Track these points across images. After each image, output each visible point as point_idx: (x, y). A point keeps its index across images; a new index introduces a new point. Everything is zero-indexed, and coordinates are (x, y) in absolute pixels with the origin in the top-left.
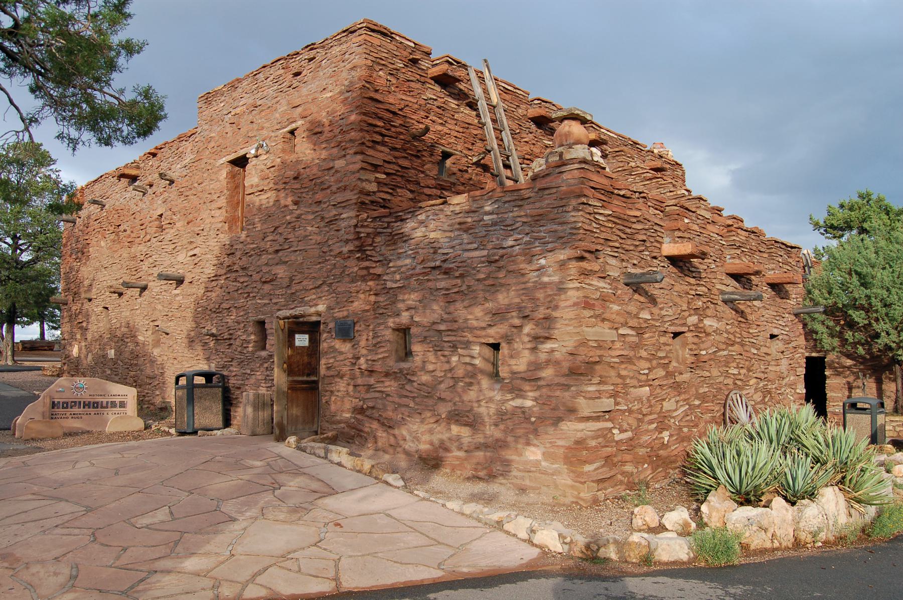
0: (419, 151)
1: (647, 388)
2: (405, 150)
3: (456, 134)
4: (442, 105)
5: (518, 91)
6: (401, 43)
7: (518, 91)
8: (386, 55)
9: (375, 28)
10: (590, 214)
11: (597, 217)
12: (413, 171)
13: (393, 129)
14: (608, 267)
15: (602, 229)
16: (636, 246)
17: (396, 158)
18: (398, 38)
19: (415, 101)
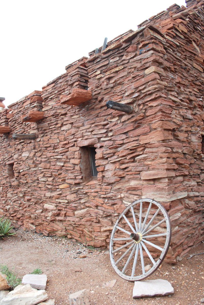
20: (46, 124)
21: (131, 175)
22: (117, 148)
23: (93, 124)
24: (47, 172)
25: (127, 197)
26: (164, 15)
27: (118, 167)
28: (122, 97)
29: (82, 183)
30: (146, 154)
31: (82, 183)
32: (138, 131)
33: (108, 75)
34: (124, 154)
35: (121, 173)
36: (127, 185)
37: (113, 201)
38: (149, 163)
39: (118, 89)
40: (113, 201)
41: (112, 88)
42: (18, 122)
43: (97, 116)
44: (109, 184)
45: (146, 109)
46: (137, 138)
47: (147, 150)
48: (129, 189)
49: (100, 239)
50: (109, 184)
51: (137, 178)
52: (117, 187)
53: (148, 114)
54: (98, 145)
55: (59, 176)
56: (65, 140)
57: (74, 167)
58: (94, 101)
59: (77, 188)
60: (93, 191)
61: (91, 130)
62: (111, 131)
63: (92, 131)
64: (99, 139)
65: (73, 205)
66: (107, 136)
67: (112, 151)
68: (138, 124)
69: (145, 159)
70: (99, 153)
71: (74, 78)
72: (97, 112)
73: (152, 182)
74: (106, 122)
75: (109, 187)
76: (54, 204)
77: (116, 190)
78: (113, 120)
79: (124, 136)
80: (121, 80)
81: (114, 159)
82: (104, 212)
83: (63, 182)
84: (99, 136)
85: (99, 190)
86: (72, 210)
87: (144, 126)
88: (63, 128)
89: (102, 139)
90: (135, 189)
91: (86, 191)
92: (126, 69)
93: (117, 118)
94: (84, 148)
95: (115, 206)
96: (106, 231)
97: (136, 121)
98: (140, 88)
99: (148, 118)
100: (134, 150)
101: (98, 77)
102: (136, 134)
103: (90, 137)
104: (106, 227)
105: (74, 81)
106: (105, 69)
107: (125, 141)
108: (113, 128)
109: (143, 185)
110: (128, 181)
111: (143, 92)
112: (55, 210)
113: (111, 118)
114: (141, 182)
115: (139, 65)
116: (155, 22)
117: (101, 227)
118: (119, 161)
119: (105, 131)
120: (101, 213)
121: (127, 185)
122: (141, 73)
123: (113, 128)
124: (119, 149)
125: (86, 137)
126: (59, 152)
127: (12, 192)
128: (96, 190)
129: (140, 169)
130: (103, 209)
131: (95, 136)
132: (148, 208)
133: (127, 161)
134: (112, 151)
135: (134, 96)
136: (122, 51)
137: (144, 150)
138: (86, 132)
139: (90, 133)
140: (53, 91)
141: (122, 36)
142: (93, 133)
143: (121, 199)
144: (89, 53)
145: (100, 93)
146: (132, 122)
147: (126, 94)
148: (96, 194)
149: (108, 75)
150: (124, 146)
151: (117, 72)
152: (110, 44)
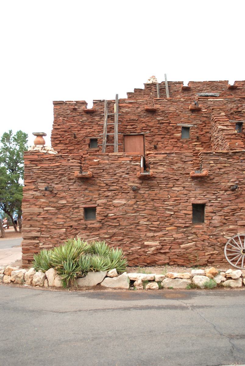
0: (78, 142)
1: (65, 229)
2: (72, 143)
3: (98, 130)
4: (91, 121)
5: (138, 101)
6: (70, 104)
7: (138, 101)
8: (62, 111)
9: (57, 103)
10: (29, 170)
11: (32, 170)
12: (75, 150)
13: (65, 137)
14: (38, 186)
15: (35, 174)
16: (57, 177)
17: (67, 147)
18: (68, 103)
19: (76, 123)
20: (155, 182)
21: (231, 222)
22: (224, 207)
23: (205, 191)
24: (153, 218)
25: (227, 234)
26: (180, 102)
27: (223, 218)
28: (229, 181)
29: (191, 226)
30: (242, 212)
31: (191, 226)
32: (237, 200)
33: (219, 166)
34: (229, 211)
35: (225, 221)
36: (227, 228)
37: (217, 237)
38: (243, 217)
39: (225, 176)
40: (217, 237)
41: (221, 174)
42: (109, 172)
43: (208, 188)
44: (215, 227)
45: (242, 191)
46: (237, 204)
47: (241, 211)
48: (228, 230)
49: (204, 260)
50: (215, 227)
51: (235, 224)
52: (220, 229)
53: (243, 193)
54: (209, 204)
55: (168, 221)
56: (177, 197)
57: (186, 215)
58: (206, 178)
59: (185, 230)
60: (201, 231)
61: (204, 194)
62: (219, 198)
63: (204, 196)
64: (210, 201)
65: (180, 241)
66: (216, 200)
67: (220, 209)
68: (237, 197)
69: (241, 215)
70: (207, 209)
71: (187, 158)
72: (209, 185)
73: (243, 227)
74: (216, 192)
75: (215, 229)
76: (158, 241)
77: (219, 231)
78: (220, 192)
79: (229, 202)
80: (228, 172)
81: (220, 213)
82: (209, 243)
83: (170, 226)
84: (210, 199)
85: (206, 230)
86: (178, 245)
87: (240, 199)
88: (173, 189)
89: (212, 201)
90: (232, 230)
91: (193, 231)
92: (232, 167)
93: (224, 192)
94: (195, 206)
95: (218, 239)
96: (209, 255)
97: (235, 196)
98: (240, 180)
99: (242, 195)
100: (235, 210)
101: (211, 165)
102: (236, 202)
103: (203, 199)
104: (210, 252)
105: (189, 160)
106: (216, 162)
107: (229, 205)
108: (221, 196)
109: (237, 228)
110: (229, 226)
111: (241, 182)
112: (159, 246)
113: (220, 191)
114: (237, 226)
115: (240, 168)
116: (171, 103)
117: (205, 252)
118: (224, 215)
119: (216, 197)
120: (207, 244)
121: (227, 228)
122: (241, 172)
123: (221, 196)
124: (225, 208)
125: (199, 198)
126: (169, 205)
127: (89, 234)
128: (203, 231)
129: (237, 219)
130: (209, 241)
131: (207, 199)
132: (239, 240)
133: (230, 215)
134: (220, 209)
135: (236, 183)
136: (229, 156)
137: (240, 210)
138: (199, 195)
139: (202, 197)
140: (164, 159)
141: (137, 101)
142: (206, 197)
143: (223, 235)
144: (94, 101)
145: (212, 174)
146: (234, 196)
147: (232, 180)
148: (203, 233)
149: (219, 166)
150: (228, 207)
151: (225, 166)
152: (123, 103)
